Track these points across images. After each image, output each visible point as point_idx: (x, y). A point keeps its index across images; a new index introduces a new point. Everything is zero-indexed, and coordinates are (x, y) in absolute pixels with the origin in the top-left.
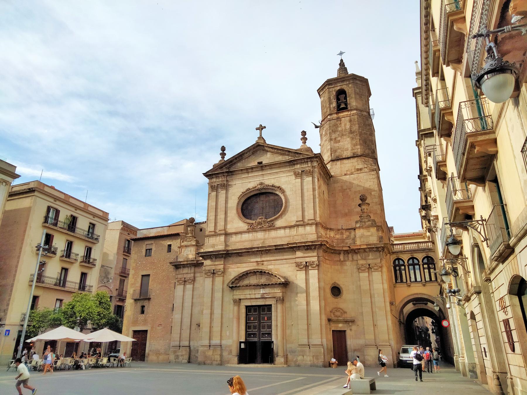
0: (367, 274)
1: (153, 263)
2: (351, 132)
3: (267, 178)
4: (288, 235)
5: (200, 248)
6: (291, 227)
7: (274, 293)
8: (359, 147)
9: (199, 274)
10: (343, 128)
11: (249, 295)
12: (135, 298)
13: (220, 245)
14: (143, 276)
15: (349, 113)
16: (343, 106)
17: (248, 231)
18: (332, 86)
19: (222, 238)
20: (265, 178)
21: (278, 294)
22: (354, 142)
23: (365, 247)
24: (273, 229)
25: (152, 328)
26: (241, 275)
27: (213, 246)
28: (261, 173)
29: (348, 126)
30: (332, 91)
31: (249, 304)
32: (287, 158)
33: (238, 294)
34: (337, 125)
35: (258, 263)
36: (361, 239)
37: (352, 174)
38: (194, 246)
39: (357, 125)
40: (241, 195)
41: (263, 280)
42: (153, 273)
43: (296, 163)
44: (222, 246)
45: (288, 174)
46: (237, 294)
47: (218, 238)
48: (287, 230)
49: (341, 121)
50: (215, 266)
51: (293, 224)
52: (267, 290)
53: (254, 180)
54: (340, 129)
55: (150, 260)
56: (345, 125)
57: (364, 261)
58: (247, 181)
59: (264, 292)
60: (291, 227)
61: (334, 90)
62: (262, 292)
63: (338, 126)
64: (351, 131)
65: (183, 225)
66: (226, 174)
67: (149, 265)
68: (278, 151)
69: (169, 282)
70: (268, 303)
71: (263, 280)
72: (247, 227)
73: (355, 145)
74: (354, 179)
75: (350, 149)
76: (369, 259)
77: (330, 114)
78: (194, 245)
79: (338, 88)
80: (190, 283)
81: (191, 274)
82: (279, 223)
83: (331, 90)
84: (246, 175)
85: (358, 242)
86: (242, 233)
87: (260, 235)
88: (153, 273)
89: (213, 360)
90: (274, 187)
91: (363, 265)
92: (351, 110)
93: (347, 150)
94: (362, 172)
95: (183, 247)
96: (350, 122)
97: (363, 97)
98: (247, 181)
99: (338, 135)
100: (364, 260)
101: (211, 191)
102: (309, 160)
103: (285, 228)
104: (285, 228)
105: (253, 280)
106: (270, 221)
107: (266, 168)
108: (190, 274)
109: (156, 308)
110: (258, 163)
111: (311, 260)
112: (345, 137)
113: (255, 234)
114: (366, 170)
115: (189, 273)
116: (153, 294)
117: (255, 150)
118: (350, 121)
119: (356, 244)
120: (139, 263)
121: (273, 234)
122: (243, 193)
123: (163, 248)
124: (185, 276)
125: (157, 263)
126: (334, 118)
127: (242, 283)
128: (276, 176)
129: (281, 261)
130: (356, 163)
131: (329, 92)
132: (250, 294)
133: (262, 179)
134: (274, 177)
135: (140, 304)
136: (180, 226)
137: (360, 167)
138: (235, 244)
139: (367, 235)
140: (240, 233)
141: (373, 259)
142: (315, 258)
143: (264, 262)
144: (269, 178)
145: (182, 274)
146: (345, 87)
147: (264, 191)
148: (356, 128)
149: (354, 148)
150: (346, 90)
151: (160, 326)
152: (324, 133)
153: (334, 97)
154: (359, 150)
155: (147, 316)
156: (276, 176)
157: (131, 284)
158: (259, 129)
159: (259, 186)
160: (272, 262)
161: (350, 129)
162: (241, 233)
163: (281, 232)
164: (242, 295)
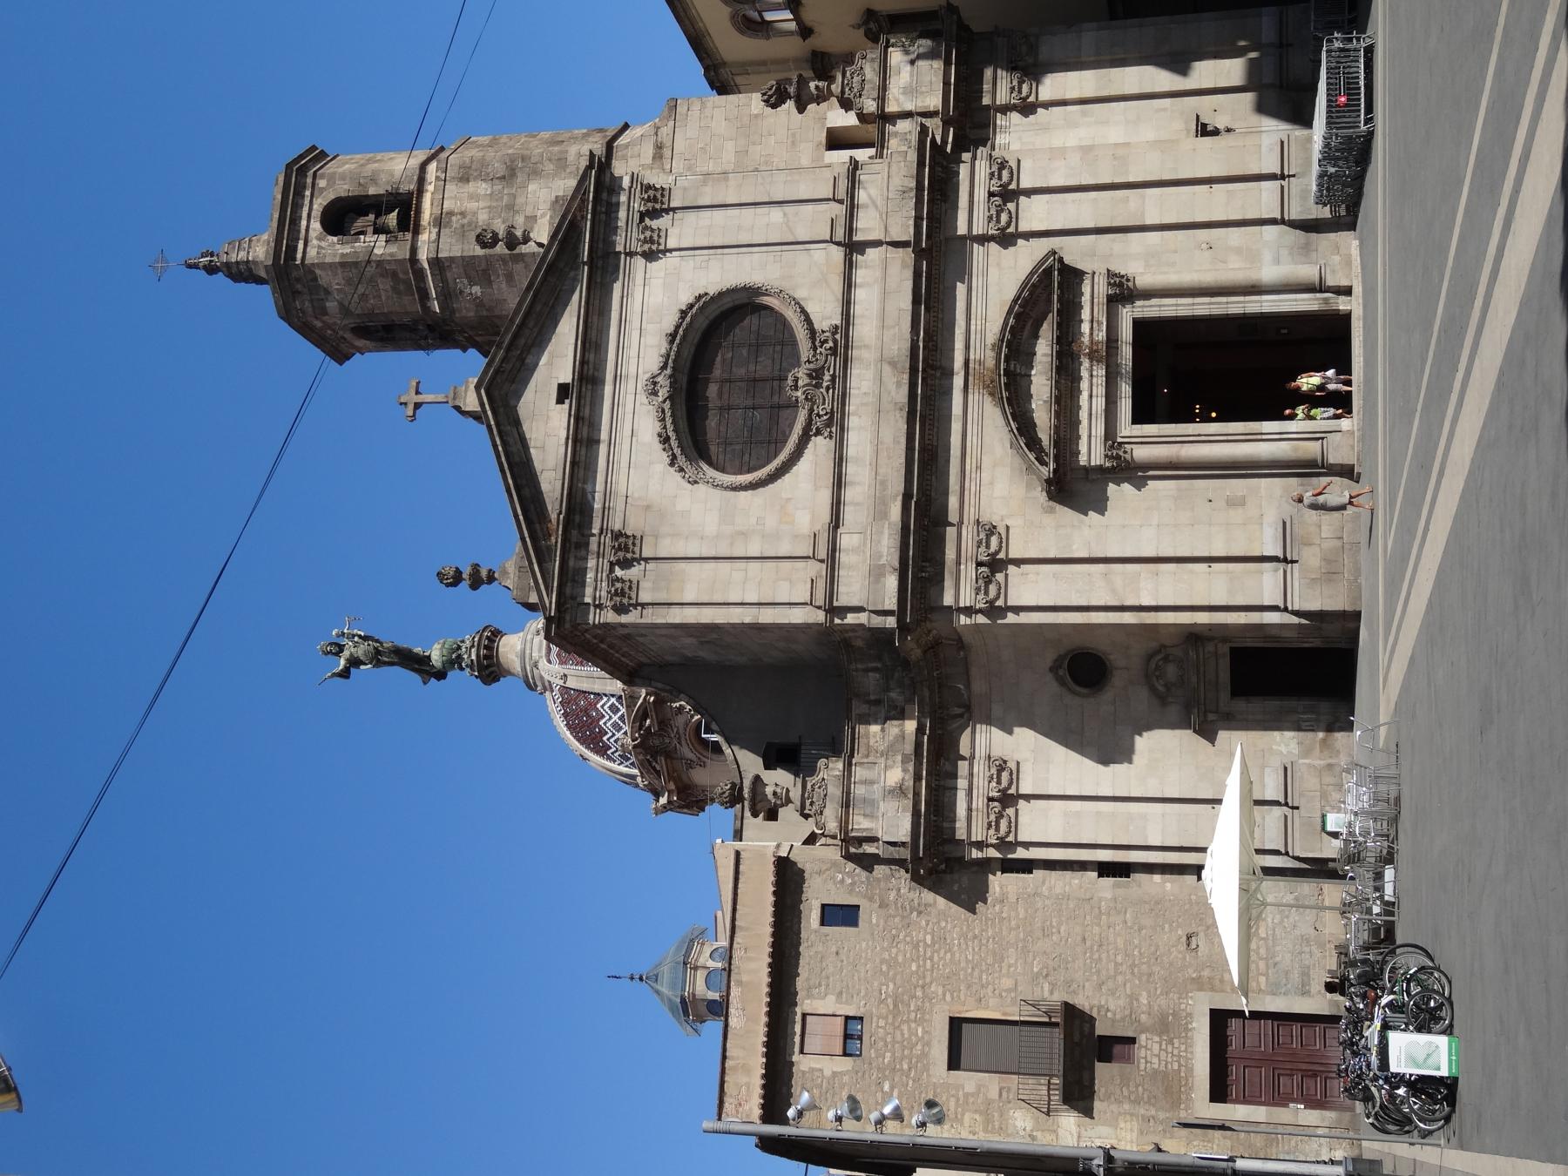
1: (895, 1006)
3: (634, 361)
4: (878, 273)
10: (482, 204)
11: (1094, 400)
13: (879, 542)
15: (431, 188)
16: (392, 219)
20: (633, 370)
22: (549, 167)
25: (1199, 984)
27: (876, 574)
29: (483, 188)
31: (1125, 407)
33: (1091, 451)
34: (463, 226)
36: (922, 93)
38: (850, 764)
40: (681, 470)
42: (948, 997)
43: (601, 245)
44: (882, 533)
47: (844, 558)
48: (860, 275)
49: (451, 213)
50: (963, 560)
53: (629, 417)
55: (882, 1023)
58: (626, 447)
61: (319, 239)
63: (470, 224)
64: (504, 177)
66: (575, 532)
69: (997, 908)
70: (1126, 332)
71: (1044, 349)
72: (819, 438)
79: (316, 226)
80: (1015, 776)
82: (825, 314)
83: (312, 252)
86: (841, 459)
87: (862, 381)
88: (948, 997)
89: (1338, 543)
92: (421, 180)
98: (626, 447)
102: (605, 196)
103: (849, 284)
104: (849, 284)
105: (1041, 385)
106: (812, 332)
107: (591, 366)
109: (1112, 973)
110: (560, 401)
111: (983, 180)
112: (520, 200)
113: (853, 405)
114: (665, 131)
116: (1046, 994)
117: (501, 410)
118: (464, 179)
120: (886, 1087)
121: (865, 330)
122: (672, 464)
123: (834, 949)
124: (979, 802)
125: (899, 982)
126: (434, 236)
128: (636, 324)
129: (974, 294)
134: (636, 334)
140: (840, 466)
143: (972, 357)
144: (634, 353)
146: (319, 204)
147: (684, 380)
149: (574, 167)
150: (332, 196)
152: (476, 290)
155: (1144, 1018)
157: (986, 1131)
158: (417, 406)
160: (973, 328)
161: (497, 182)
162: (839, 460)
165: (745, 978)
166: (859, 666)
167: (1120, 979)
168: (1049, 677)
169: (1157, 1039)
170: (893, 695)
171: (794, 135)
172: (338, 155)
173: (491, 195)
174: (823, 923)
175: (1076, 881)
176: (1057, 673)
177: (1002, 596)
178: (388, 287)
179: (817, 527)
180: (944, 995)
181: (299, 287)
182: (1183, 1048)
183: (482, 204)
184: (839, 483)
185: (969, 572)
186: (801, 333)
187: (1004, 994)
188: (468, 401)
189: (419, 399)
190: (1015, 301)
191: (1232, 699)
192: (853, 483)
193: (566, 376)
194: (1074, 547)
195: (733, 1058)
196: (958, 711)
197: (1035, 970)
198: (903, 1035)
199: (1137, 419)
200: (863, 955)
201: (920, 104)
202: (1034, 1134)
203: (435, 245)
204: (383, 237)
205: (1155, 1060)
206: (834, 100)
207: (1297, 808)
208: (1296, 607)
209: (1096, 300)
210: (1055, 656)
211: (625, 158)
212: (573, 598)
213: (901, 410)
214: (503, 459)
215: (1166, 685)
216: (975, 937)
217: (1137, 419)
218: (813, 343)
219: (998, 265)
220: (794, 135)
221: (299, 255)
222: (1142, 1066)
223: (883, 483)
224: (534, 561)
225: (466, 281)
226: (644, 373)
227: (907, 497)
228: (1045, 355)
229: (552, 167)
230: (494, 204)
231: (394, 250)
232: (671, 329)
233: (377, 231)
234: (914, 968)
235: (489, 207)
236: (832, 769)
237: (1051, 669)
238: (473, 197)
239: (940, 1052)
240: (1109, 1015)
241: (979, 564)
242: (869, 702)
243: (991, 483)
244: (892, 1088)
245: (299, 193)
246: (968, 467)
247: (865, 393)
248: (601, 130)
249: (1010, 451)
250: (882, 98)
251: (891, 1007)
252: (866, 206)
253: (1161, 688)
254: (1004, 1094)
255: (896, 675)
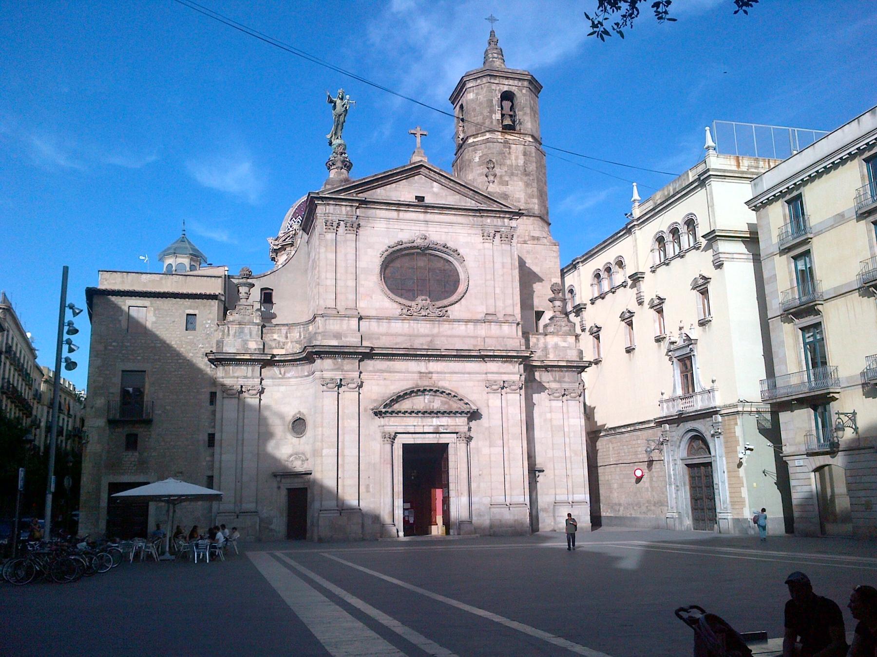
0: (560, 404)
2: (526, 173)
4: (471, 335)
5: (270, 331)
6: (477, 322)
7: (456, 425)
8: (536, 201)
9: (271, 380)
10: (514, 161)
11: (413, 427)
12: (111, 417)
13: (352, 337)
14: (123, 371)
17: (401, 318)
18: (496, 82)
19: (354, 322)
20: (430, 229)
21: (463, 427)
22: (529, 191)
23: (565, 364)
24: (447, 321)
26: (402, 394)
27: (337, 336)
28: (421, 216)
29: (521, 162)
30: (496, 90)
32: (470, 204)
34: (504, 153)
35: (422, 374)
36: (555, 352)
37: (525, 242)
38: (258, 325)
39: (534, 164)
41: (437, 403)
44: (356, 338)
45: (470, 231)
46: (391, 424)
48: (471, 326)
49: (510, 148)
50: (343, 373)
51: (480, 316)
52: (444, 421)
54: (508, 162)
56: (517, 158)
57: (559, 384)
58: (396, 227)
59: (439, 424)
60: (476, 321)
61: (500, 89)
62: (434, 424)
63: (505, 156)
64: (526, 171)
65: (220, 279)
67: (141, 351)
68: (454, 186)
70: (443, 439)
71: (437, 403)
73: (531, 196)
74: (528, 252)
75: (523, 201)
76: (565, 382)
77: (491, 131)
78: (258, 325)
79: (506, 88)
81: (256, 380)
82: (455, 311)
83: (494, 87)
84: (394, 214)
85: (551, 356)
90: (447, 248)
91: (557, 390)
93: (519, 202)
94: (539, 243)
95: (232, 324)
96: (524, 155)
97: (536, 116)
99: (506, 171)
100: (559, 382)
101: (325, 230)
102: (507, 216)
103: (467, 321)
105: (420, 402)
108: (251, 379)
110: (417, 197)
112: (515, 178)
114: (545, 241)
115: (249, 378)
118: (525, 154)
119: (549, 357)
120: (114, 344)
121: (445, 328)
122: (389, 247)
123: (176, 320)
126: (500, 140)
127: (396, 407)
128: (451, 230)
129: (462, 375)
130: (531, 227)
131: (491, 91)
132: (415, 426)
133: (426, 229)
135: (122, 432)
136: (213, 278)
137: (537, 234)
138: (379, 338)
139: (563, 347)
141: (570, 383)
142: (516, 375)
143: (434, 375)
145: (234, 377)
146: (514, 89)
148: (532, 167)
151: (178, 475)
152: (477, 159)
153: (498, 101)
154: (536, 207)
155: (146, 454)
156: (451, 230)
159: (419, 241)
160: (447, 375)
162: (389, 319)
163: (461, 329)
164: (401, 426)
165: (164, 282)
166: (302, 329)
167: (163, 444)
168: (297, 411)
169: (136, 460)
170: (289, 343)
171: (542, 297)
172: (538, 97)
173: (518, 166)
174: (187, 315)
175: (206, 424)
176: (298, 414)
177: (328, 390)
178: (478, 121)
179: (360, 311)
180: (156, 368)
181: (479, 81)
182: (133, 471)
183: (514, 161)
184: (379, 319)
185: (338, 375)
186: (446, 302)
187: (156, 394)
188: (417, 157)
189: (418, 135)
190: (456, 393)
191: (287, 489)
192: (379, 326)
193: (428, 200)
194: (349, 421)
195: (127, 277)
196: (282, 372)
197: (167, 407)
198: (138, 350)
199: (405, 446)
200: (174, 333)
201: (550, 351)
202: (94, 408)
203: (495, 140)
204: (500, 118)
205: (126, 460)
206: (554, 314)
207: (237, 518)
208: (321, 515)
209: (457, 427)
210: (305, 413)
211: (533, 224)
212: (328, 204)
213: (411, 345)
214: (390, 173)
215: (292, 461)
216: (181, 381)
217: (405, 446)
218: (442, 307)
219: (474, 386)
220: (542, 297)
221: (492, 81)
222: (124, 453)
223: (379, 338)
224: (344, 187)
225: (481, 155)
226: (429, 235)
227: (372, 349)
228: (433, 406)
229: (530, 192)
230: (513, 167)
231: (494, 123)
232: (448, 245)
233: (503, 115)
234: (169, 355)
235: (512, 165)
236: (256, 319)
237: (300, 412)
238: (517, 158)
239: (130, 366)
240: (147, 439)
241: (341, 380)
242: (287, 333)
243: (378, 385)
244: (114, 346)
245: (520, 79)
246: (385, 374)
247: (418, 330)
248: (547, 213)
249: (392, 392)
250: (552, 333)
251: (150, 345)
252: (501, 329)
253: (291, 459)
254: (111, 395)
255: (297, 345)
